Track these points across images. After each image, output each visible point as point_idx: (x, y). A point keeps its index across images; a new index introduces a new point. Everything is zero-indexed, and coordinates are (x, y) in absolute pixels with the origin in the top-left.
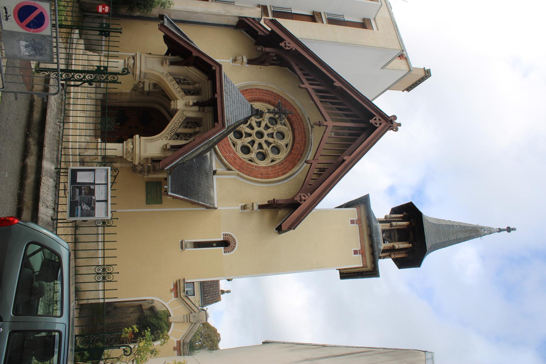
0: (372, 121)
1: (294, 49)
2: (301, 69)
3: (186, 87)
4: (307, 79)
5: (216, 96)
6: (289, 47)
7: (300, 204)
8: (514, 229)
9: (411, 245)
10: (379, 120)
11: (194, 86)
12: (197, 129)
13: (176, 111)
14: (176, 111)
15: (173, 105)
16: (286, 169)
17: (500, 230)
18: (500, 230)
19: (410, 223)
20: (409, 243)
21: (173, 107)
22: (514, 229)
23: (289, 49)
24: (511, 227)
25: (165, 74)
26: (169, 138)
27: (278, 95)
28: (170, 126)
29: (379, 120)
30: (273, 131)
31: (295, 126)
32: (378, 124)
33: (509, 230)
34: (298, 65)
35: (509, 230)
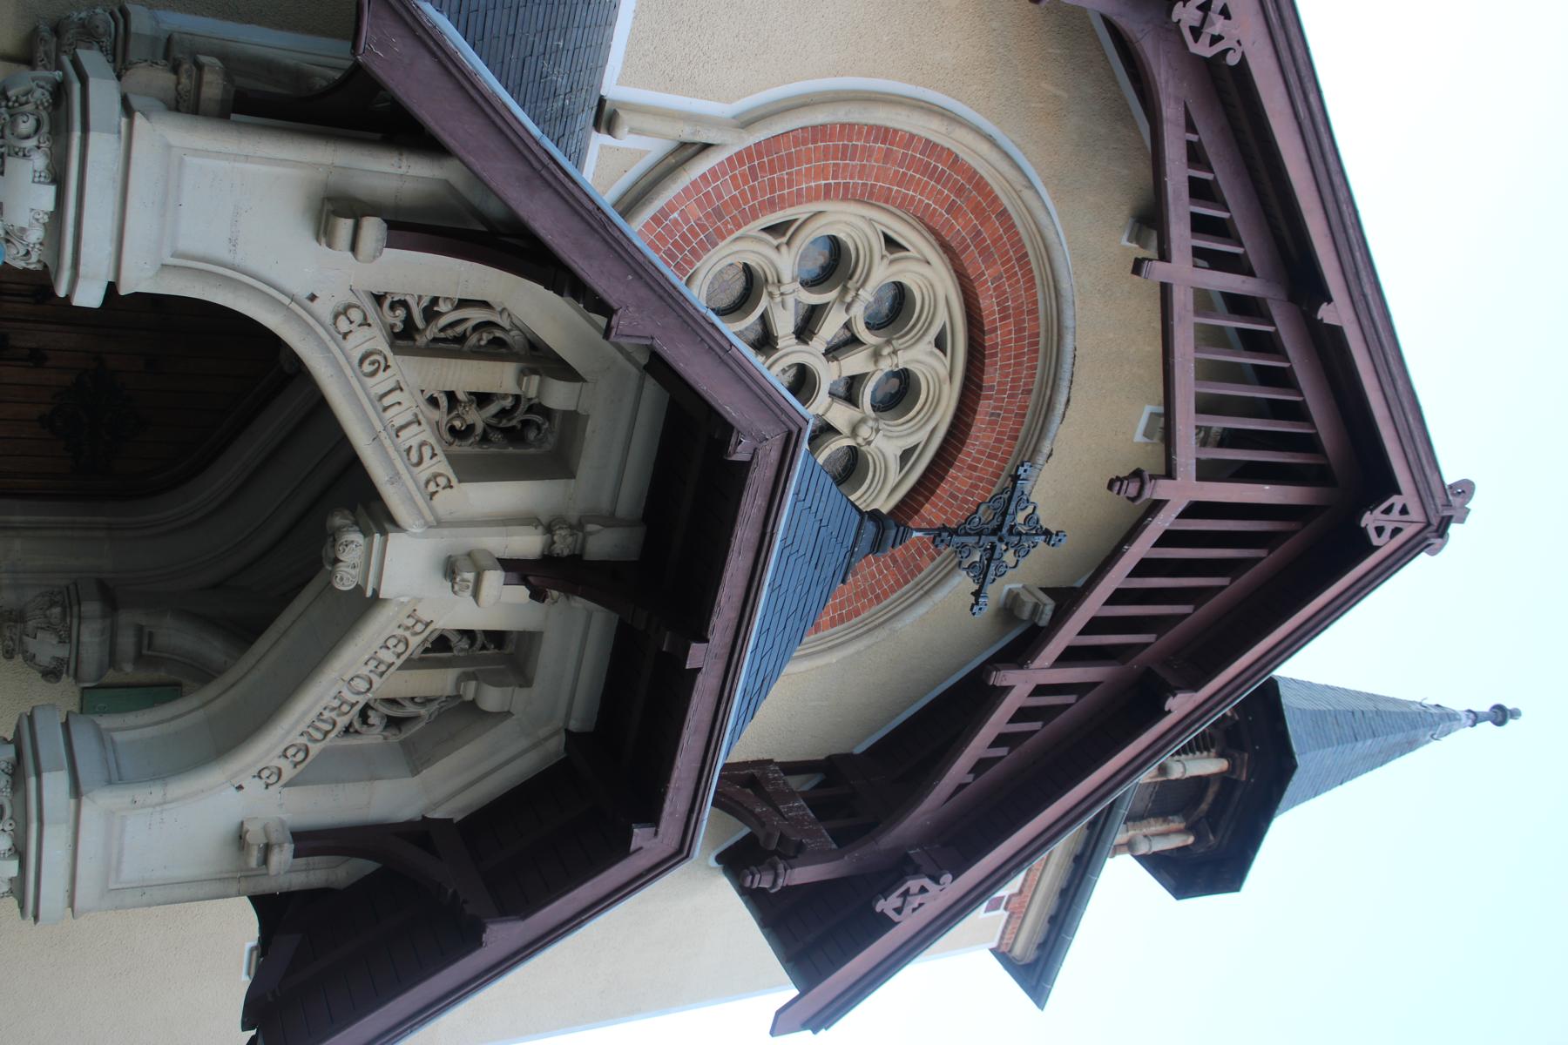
0: (1369, 520)
1: (1232, 59)
2: (1195, 155)
3: (467, 375)
4: (1200, 225)
5: (697, 655)
6: (1215, 39)
7: (893, 924)
8: (1515, 714)
9: (1191, 840)
10: (1404, 511)
11: (532, 385)
12: (492, 698)
13: (364, 603)
14: (364, 603)
15: (352, 556)
16: (864, 594)
17: (1476, 718)
18: (1476, 718)
19: (1232, 767)
20: (1189, 829)
21: (346, 578)
22: (1515, 714)
23: (1209, 52)
24: (1509, 706)
25: (324, 308)
26: (288, 772)
27: (981, 185)
28: (305, 714)
29: (1404, 511)
30: (870, 368)
31: (992, 376)
32: (1387, 532)
33: (1500, 715)
34: (1190, 127)
35: (1500, 715)
